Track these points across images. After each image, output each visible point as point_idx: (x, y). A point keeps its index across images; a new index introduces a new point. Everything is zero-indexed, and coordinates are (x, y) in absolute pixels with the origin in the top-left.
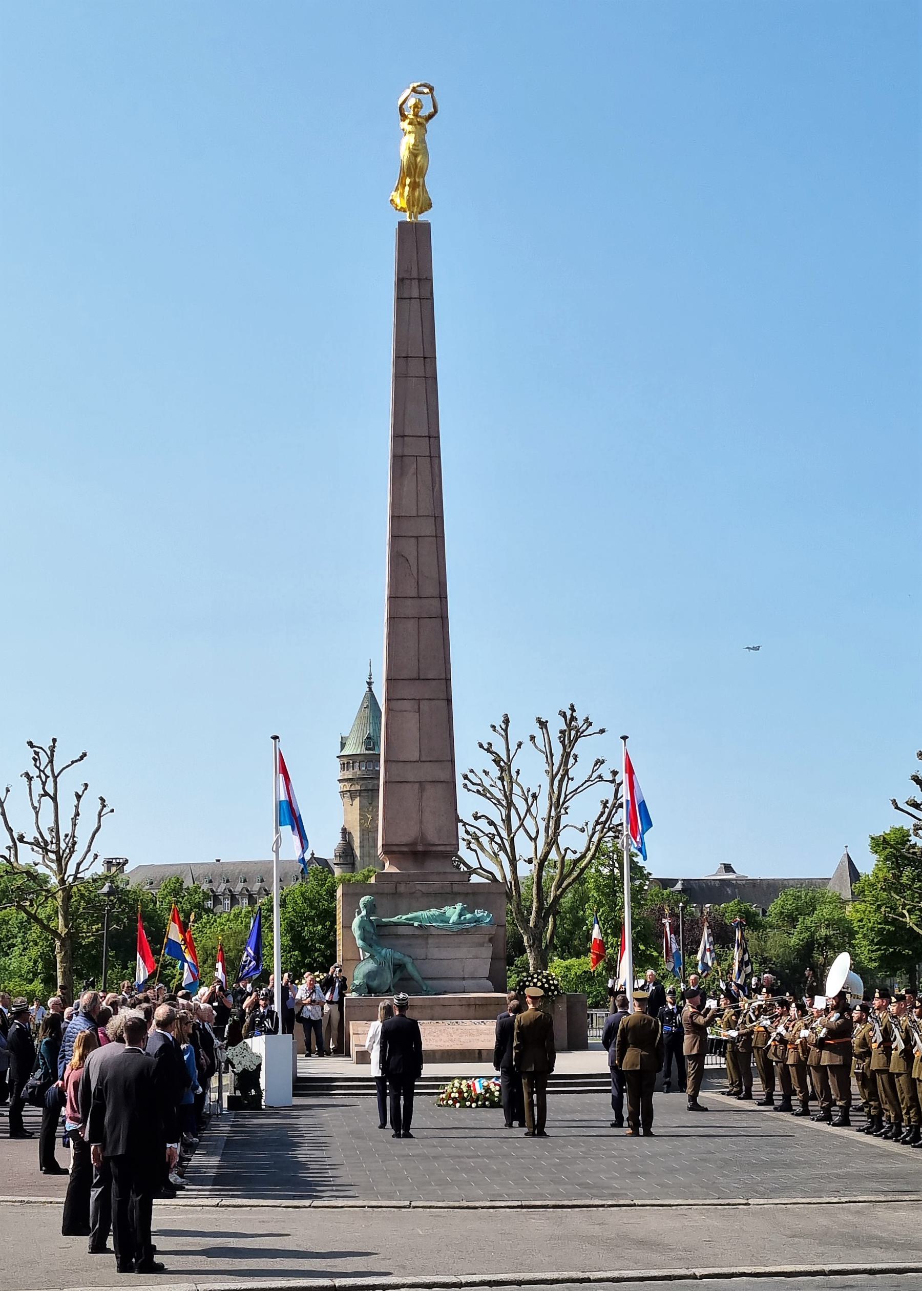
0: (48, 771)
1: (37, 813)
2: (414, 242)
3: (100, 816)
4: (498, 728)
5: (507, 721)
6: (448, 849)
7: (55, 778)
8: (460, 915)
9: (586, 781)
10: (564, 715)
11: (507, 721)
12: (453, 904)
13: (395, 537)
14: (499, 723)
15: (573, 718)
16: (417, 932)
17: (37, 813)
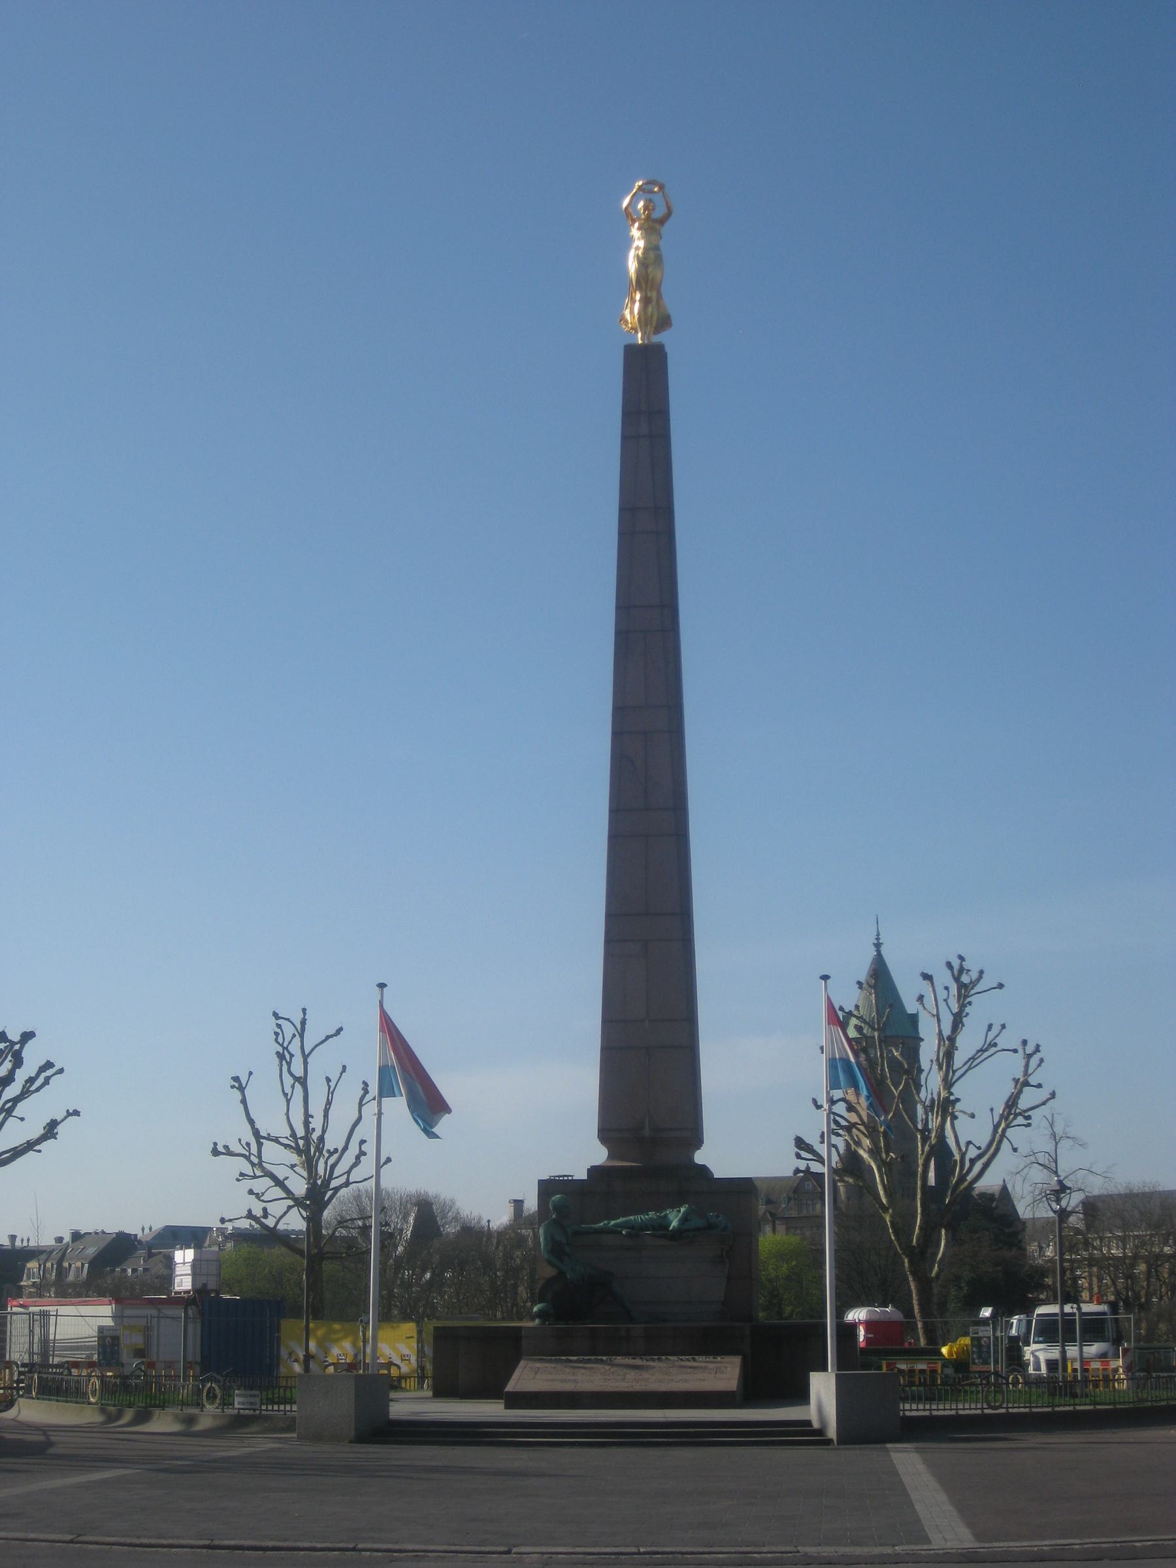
0: (295, 1048)
1: (288, 1101)
2: (645, 370)
3: (361, 1105)
7: (305, 1057)
10: (949, 965)
12: (675, 1205)
13: (618, 734)
15: (961, 970)
17: (288, 1101)
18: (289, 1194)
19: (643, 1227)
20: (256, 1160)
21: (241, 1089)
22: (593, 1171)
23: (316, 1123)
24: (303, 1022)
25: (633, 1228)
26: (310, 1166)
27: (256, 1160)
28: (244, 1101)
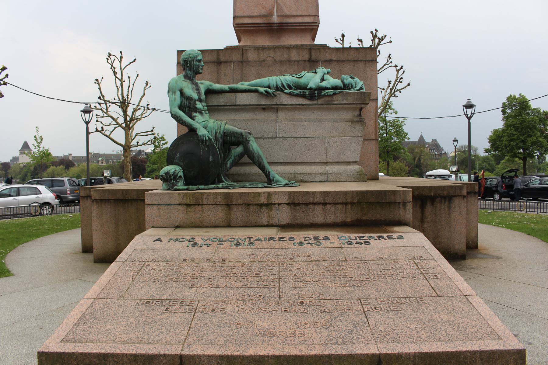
3: (145, 89)
4: (339, 40)
5: (343, 36)
6: (307, 20)
8: (323, 80)
9: (385, 65)
10: (372, 33)
11: (343, 36)
14: (339, 37)
16: (264, 102)
18: (117, 123)
19: (279, 89)
20: (105, 111)
21: (99, 84)
22: (230, 49)
23: (125, 94)
24: (121, 58)
25: (269, 87)
26: (125, 112)
27: (105, 111)
28: (100, 89)
